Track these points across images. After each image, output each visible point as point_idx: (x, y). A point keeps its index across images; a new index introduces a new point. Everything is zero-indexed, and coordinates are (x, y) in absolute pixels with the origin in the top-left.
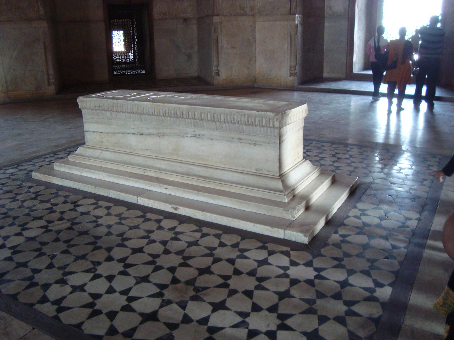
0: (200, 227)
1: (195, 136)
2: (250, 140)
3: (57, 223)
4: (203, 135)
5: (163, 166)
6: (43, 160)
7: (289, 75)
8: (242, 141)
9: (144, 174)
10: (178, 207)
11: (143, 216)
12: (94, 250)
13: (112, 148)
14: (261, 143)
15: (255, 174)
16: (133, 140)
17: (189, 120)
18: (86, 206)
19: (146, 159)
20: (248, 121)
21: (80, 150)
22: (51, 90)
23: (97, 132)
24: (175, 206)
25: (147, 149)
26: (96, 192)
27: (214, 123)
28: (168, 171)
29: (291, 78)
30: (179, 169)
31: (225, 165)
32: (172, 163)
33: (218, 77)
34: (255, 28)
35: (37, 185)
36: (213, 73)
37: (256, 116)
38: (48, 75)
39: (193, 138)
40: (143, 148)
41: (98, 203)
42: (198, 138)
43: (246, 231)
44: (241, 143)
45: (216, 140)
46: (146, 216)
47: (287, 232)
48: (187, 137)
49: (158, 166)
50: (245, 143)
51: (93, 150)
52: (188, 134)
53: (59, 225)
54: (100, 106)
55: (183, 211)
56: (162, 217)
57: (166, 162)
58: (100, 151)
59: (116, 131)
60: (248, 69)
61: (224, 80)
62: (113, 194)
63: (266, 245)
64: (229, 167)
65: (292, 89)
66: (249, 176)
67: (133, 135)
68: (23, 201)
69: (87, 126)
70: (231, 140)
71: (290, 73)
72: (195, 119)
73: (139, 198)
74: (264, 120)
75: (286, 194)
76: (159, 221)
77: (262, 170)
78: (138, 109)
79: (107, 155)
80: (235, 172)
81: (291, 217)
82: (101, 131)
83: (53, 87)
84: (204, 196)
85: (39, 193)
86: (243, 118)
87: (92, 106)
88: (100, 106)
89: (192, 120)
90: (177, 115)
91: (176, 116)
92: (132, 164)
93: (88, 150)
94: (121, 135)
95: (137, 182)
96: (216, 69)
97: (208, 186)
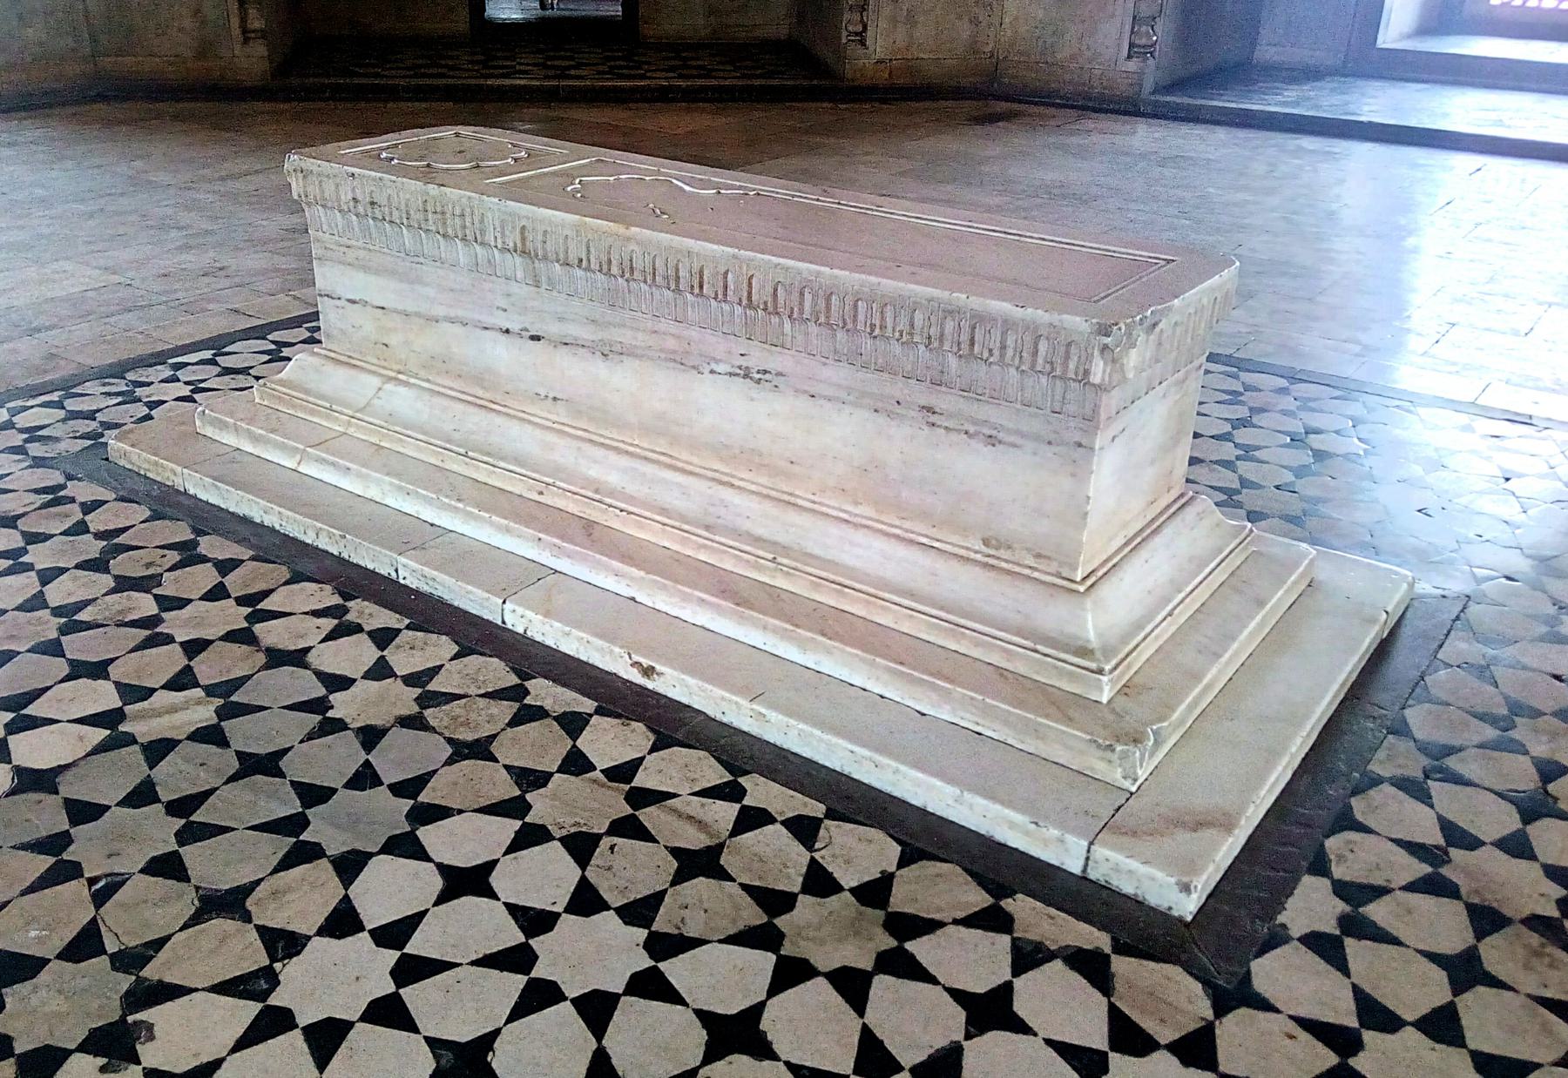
0: (736, 770)
2: (975, 422)
3: (163, 698)
4: (779, 374)
5: (613, 479)
6: (168, 373)
7: (1125, 52)
8: (933, 418)
10: (658, 667)
11: (516, 693)
12: (286, 864)
13: (422, 374)
14: (1019, 441)
15: (978, 557)
16: (502, 355)
17: (726, 307)
19: (551, 438)
20: (972, 344)
21: (301, 363)
22: (251, 60)
24: (645, 662)
27: (825, 331)
28: (631, 499)
31: (856, 503)
32: (649, 469)
33: (860, 51)
35: (123, 499)
36: (844, 33)
41: (346, 611)
43: (923, 812)
46: (527, 693)
48: (712, 372)
49: (594, 472)
51: (353, 372)
52: (717, 361)
53: (173, 710)
54: (372, 203)
55: (674, 684)
56: (588, 705)
57: (625, 461)
58: (375, 381)
59: (440, 311)
60: (975, 22)
61: (880, 62)
62: (411, 573)
63: (1008, 904)
64: (873, 514)
65: (1128, 107)
66: (955, 565)
67: (504, 337)
68: (47, 577)
69: (327, 277)
72: (750, 305)
75: (1108, 668)
76: (573, 724)
79: (402, 401)
80: (897, 537)
81: (1119, 773)
83: (259, 49)
85: (122, 539)
86: (950, 326)
87: (346, 196)
89: (739, 310)
90: (678, 278)
91: (674, 282)
92: (492, 455)
93: (330, 368)
94: (457, 329)
95: (508, 530)
96: (857, 17)
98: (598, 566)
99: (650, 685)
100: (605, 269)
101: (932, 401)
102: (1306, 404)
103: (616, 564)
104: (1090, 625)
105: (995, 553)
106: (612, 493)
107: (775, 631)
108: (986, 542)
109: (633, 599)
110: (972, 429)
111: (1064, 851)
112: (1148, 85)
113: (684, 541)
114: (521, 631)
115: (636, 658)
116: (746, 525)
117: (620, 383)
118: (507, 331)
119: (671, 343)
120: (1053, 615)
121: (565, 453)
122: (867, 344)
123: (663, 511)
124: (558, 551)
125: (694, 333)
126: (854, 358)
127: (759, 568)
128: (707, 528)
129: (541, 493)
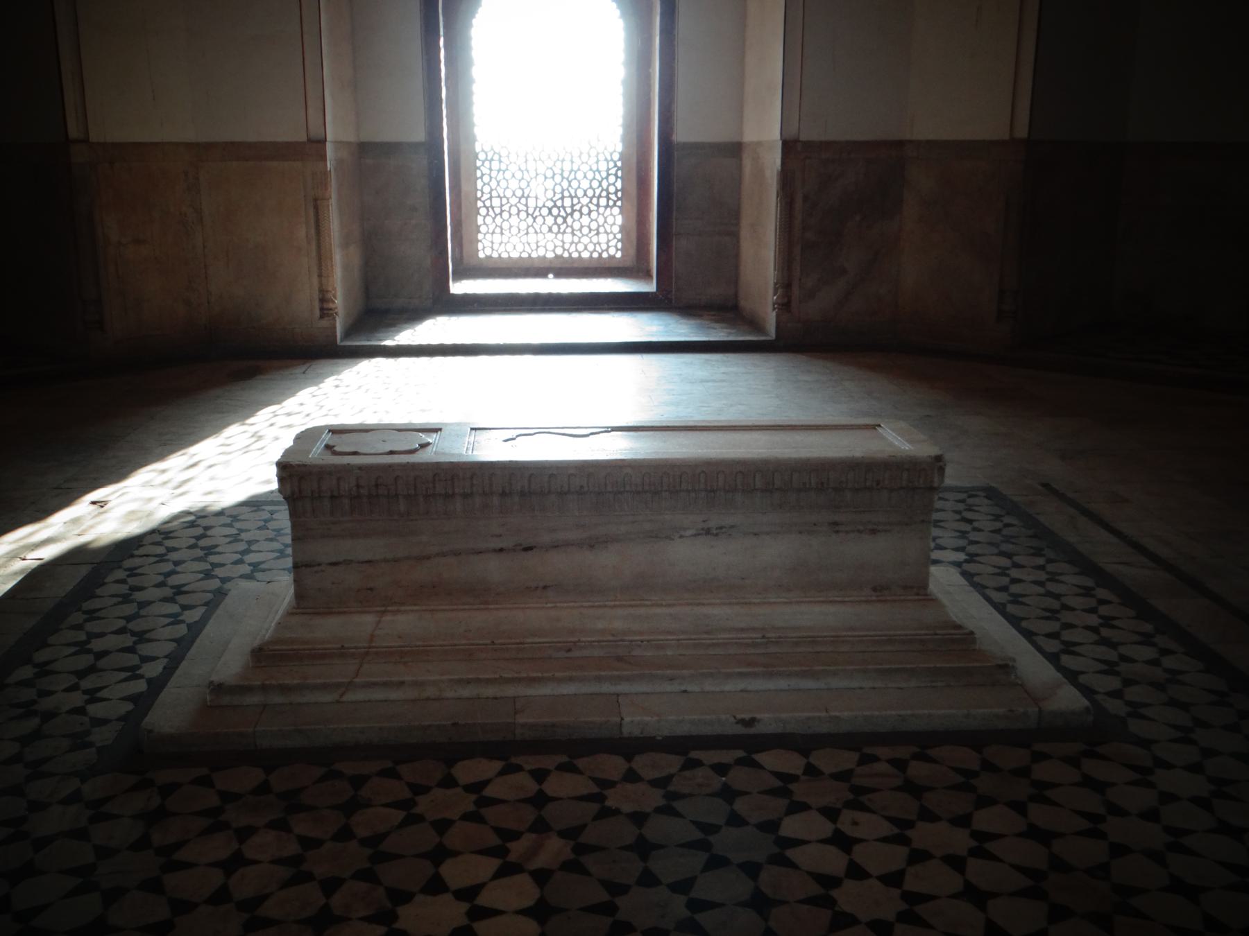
1: (708, 532)
4: (732, 527)
7: (317, 313)
8: (837, 528)
10: (758, 716)
23: (348, 562)
24: (747, 716)
25: (545, 587)
42: (717, 535)
44: (837, 532)
45: (768, 533)
48: (681, 537)
50: (847, 532)
52: (685, 529)
58: (369, 619)
82: (368, 557)
88: (377, 485)
99: (752, 731)
108: (875, 589)
109: (685, 691)
110: (861, 528)
115: (739, 716)
118: (501, 550)
128: (707, 633)
129: (569, 650)
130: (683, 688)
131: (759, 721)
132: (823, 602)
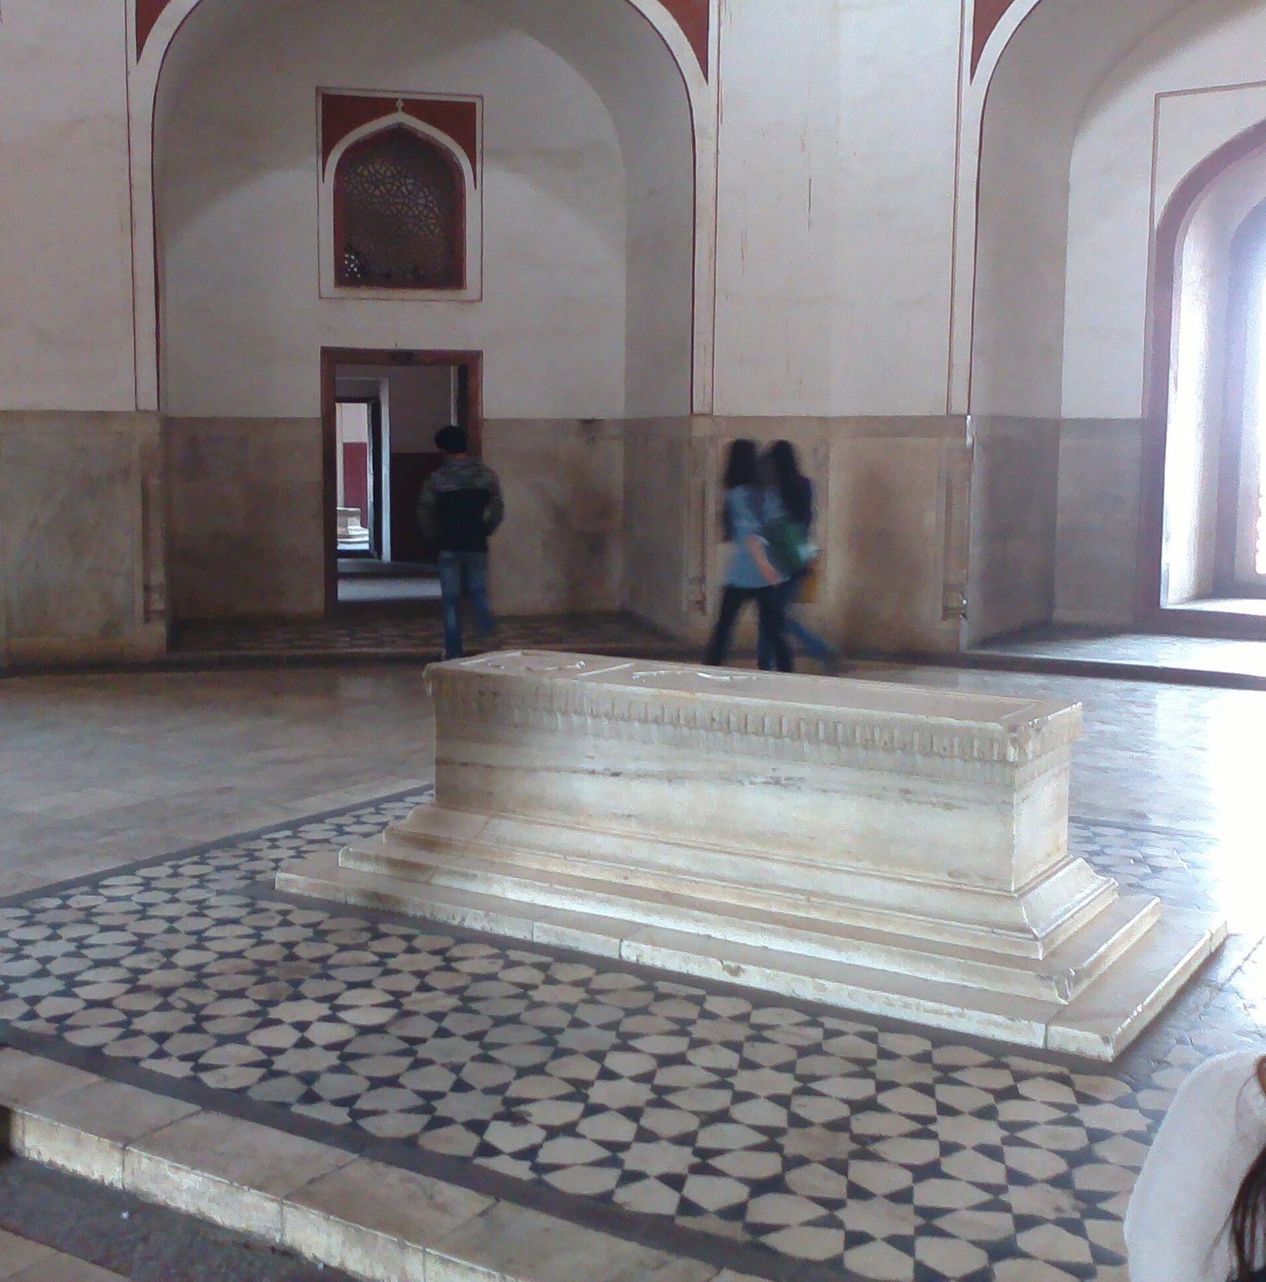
1: (777, 782)
2: (936, 795)
4: (801, 779)
5: (680, 864)
7: (940, 613)
9: (627, 882)
10: (743, 967)
17: (762, 739)
18: (476, 960)
19: (626, 841)
24: (733, 965)
25: (629, 816)
26: (488, 929)
28: (697, 874)
29: (947, 625)
30: (728, 872)
31: (859, 860)
34: (827, 456)
37: (953, 731)
38: (147, 588)
39: (772, 788)
40: (619, 812)
42: (785, 786)
44: (909, 801)
47: (1054, 1029)
48: (752, 783)
49: (664, 860)
50: (920, 803)
55: (754, 978)
62: (542, 934)
70: (879, 795)
71: (946, 609)
73: (625, 943)
74: (976, 743)
77: (966, 876)
78: (613, 705)
84: (810, 940)
89: (772, 740)
91: (726, 728)
95: (609, 902)
97: (814, 915)
98: (681, 917)
100: (675, 723)
101: (910, 785)
102: (1140, 843)
103: (696, 913)
104: (1025, 915)
105: (958, 880)
106: (680, 871)
107: (818, 941)
108: (950, 874)
110: (935, 800)
111: (1032, 1035)
112: (964, 639)
113: (740, 897)
114: (633, 959)
116: (784, 883)
117: (680, 800)
118: (593, 772)
119: (720, 767)
120: (999, 912)
121: (640, 851)
122: (861, 754)
123: (721, 879)
124: (648, 912)
125: (739, 760)
126: (850, 764)
127: (796, 907)
129: (626, 878)
130: (707, 932)
131: (743, 971)
132: (890, 879)
